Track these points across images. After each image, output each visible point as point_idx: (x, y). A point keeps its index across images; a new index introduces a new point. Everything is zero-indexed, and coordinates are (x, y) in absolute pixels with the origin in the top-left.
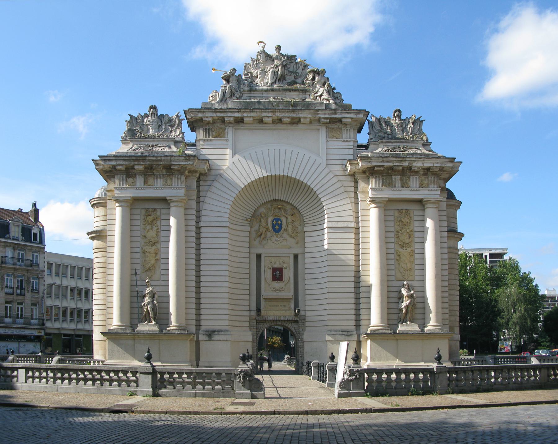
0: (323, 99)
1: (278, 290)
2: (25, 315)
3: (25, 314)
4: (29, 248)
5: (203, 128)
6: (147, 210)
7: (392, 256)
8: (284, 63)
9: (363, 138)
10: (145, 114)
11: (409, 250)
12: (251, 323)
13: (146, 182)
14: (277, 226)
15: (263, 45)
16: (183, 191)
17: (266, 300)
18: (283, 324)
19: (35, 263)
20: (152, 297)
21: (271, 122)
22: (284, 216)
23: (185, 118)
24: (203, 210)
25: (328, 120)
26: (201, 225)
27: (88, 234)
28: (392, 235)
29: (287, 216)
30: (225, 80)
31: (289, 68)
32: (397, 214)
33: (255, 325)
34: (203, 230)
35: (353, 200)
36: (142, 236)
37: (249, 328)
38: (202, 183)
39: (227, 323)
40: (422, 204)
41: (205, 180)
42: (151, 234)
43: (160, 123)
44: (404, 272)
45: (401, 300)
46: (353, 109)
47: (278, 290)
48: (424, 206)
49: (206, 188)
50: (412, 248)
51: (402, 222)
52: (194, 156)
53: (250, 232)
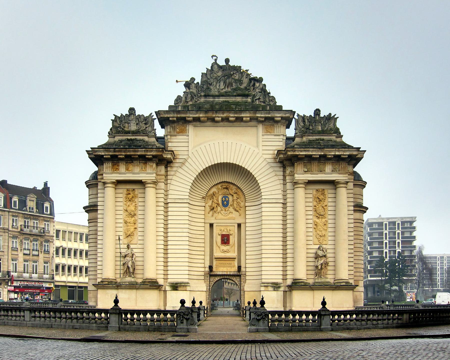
0: (261, 102)
2: (39, 271)
3: (39, 270)
4: (42, 218)
5: (169, 126)
6: (128, 190)
7: (311, 226)
9: (291, 132)
10: (126, 115)
11: (324, 220)
12: (205, 277)
13: (127, 169)
14: (225, 202)
15: (215, 58)
16: (154, 175)
17: (217, 259)
18: (229, 278)
19: (46, 230)
20: (132, 256)
21: (221, 121)
22: (231, 194)
23: (156, 118)
24: (170, 190)
25: (264, 119)
26: (169, 202)
27: (84, 208)
28: (311, 209)
29: (233, 194)
30: (187, 87)
31: (235, 77)
32: (315, 193)
34: (170, 205)
35: (282, 182)
36: (125, 210)
37: (203, 280)
38: (169, 169)
39: (187, 277)
40: (334, 184)
41: (171, 167)
42: (132, 208)
43: (137, 122)
44: (320, 238)
45: (317, 260)
46: (283, 109)
48: (335, 186)
49: (172, 173)
50: (326, 220)
51: (319, 198)
52: (163, 148)
53: (205, 207)
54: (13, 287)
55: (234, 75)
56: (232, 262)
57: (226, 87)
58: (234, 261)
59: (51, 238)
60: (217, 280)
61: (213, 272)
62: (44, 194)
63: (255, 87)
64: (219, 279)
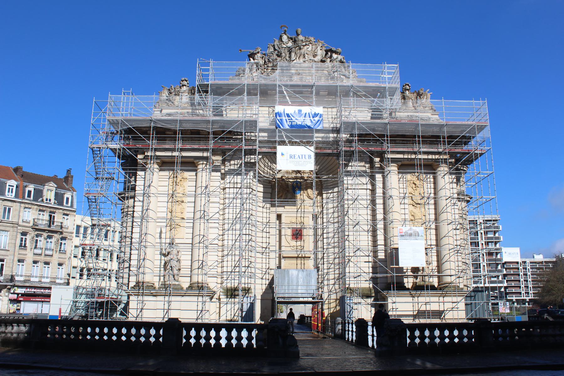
8: (304, 44)
54: (16, 295)
55: (307, 46)
57: (297, 58)
59: (70, 234)
62: (65, 183)
63: (332, 58)
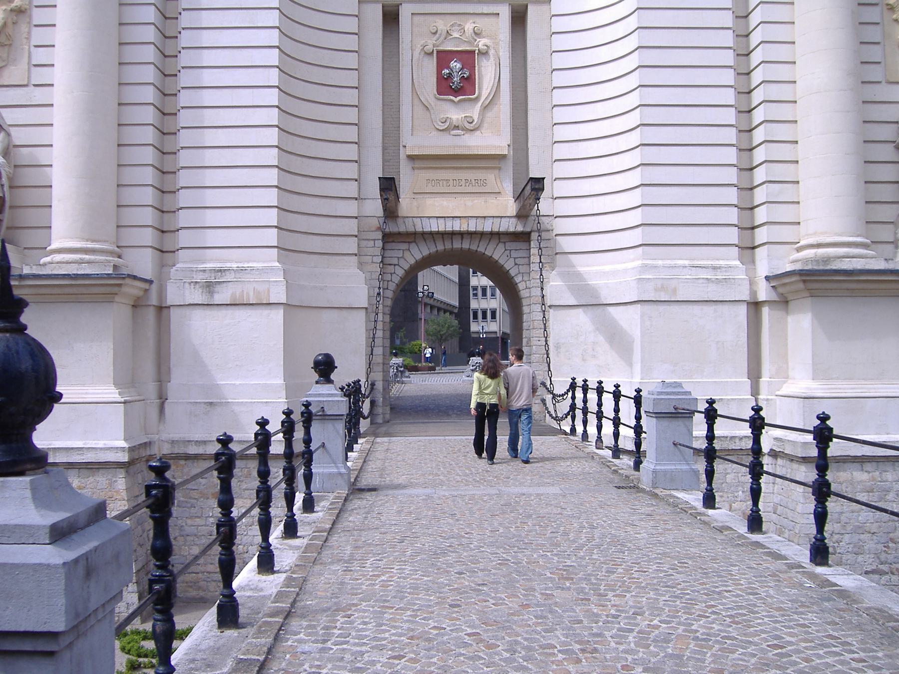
1: (457, 127)
12: (364, 243)
17: (418, 164)
33: (378, 251)
37: (355, 259)
47: (457, 127)
56: (490, 176)
58: (500, 169)
60: (419, 257)
61: (400, 221)
64: (426, 252)
